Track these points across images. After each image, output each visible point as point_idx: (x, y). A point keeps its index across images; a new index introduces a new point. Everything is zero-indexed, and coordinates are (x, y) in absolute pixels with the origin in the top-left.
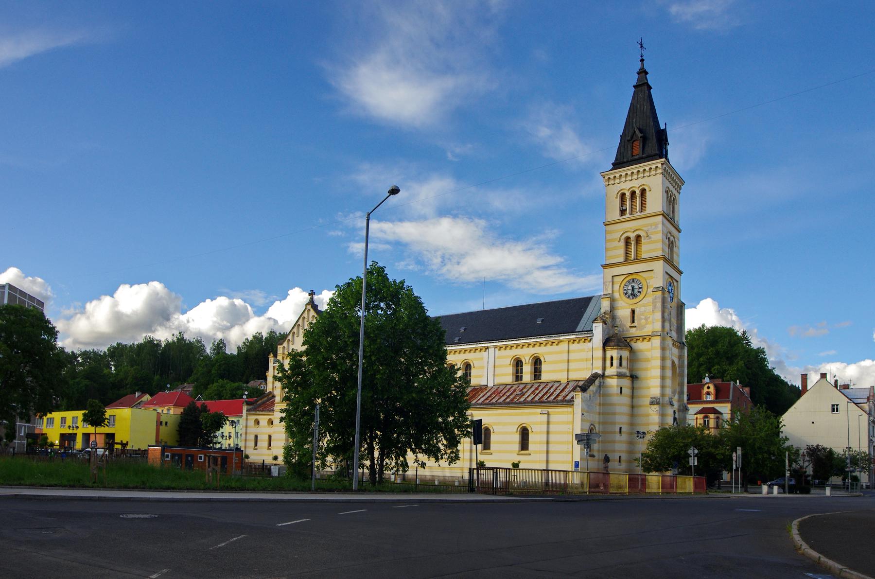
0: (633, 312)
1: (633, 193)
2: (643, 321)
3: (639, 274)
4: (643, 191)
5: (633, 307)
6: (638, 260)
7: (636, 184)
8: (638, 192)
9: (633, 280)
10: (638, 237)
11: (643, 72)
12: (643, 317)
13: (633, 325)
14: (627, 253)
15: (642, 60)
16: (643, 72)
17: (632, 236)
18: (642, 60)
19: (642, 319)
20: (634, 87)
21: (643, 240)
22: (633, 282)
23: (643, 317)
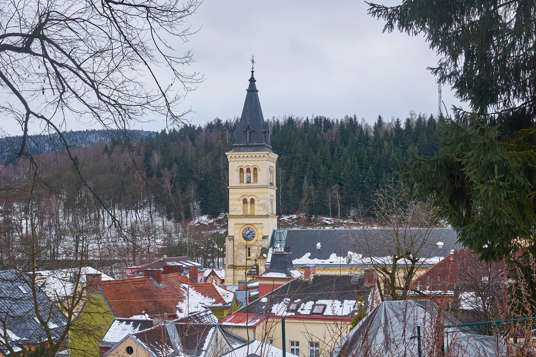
4: (255, 169)
6: (252, 216)
7: (251, 164)
11: (252, 80)
13: (249, 257)
14: (244, 210)
15: (253, 72)
16: (252, 80)
18: (253, 72)
21: (256, 202)
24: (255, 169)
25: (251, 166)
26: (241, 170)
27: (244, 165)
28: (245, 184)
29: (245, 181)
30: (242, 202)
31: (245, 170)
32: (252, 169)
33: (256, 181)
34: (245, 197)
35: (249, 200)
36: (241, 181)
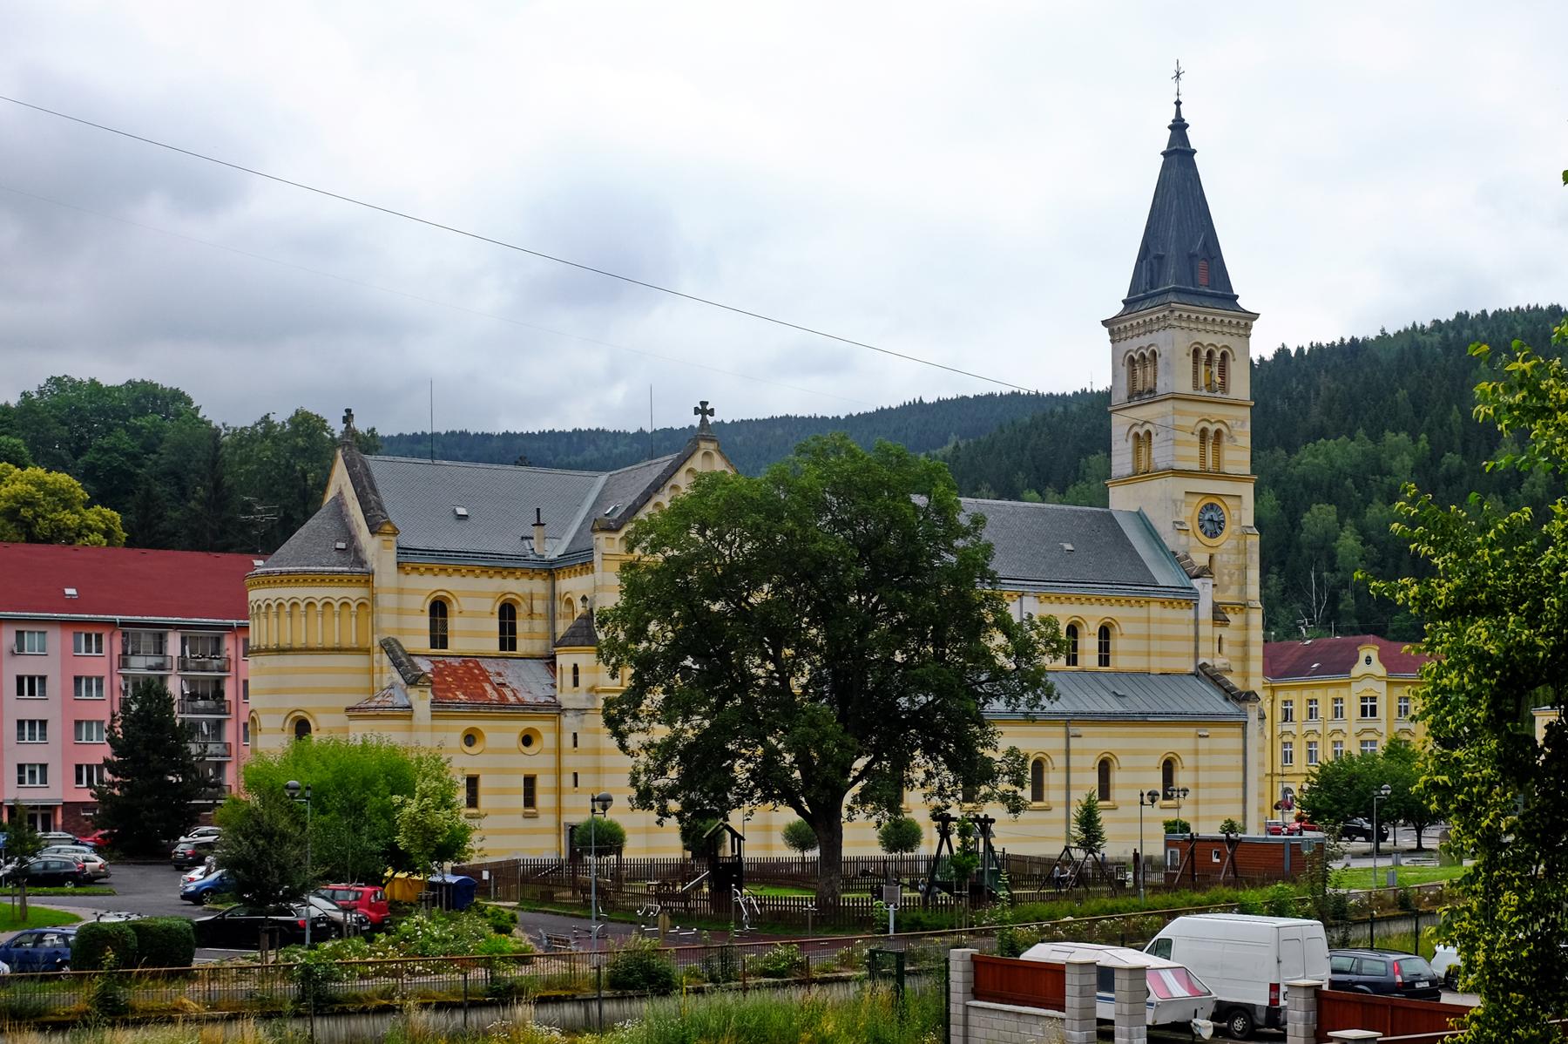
0: (1211, 557)
1: (1210, 354)
2: (1226, 578)
3: (1223, 498)
5: (1212, 551)
6: (1219, 475)
7: (1219, 341)
8: (1218, 355)
9: (1212, 505)
10: (1218, 433)
12: (1226, 571)
14: (1203, 457)
15: (1178, 103)
17: (1212, 428)
18: (1178, 103)
19: (1224, 574)
20: (1163, 153)
21: (1225, 438)
22: (1212, 508)
23: (1226, 571)
24: (1224, 355)
25: (1219, 346)
26: (1196, 353)
27: (1207, 339)
28: (1204, 392)
29: (1202, 383)
30: (1196, 439)
31: (1204, 353)
32: (1218, 355)
33: (1224, 387)
34: (1206, 424)
35: (1211, 433)
36: (1196, 386)
